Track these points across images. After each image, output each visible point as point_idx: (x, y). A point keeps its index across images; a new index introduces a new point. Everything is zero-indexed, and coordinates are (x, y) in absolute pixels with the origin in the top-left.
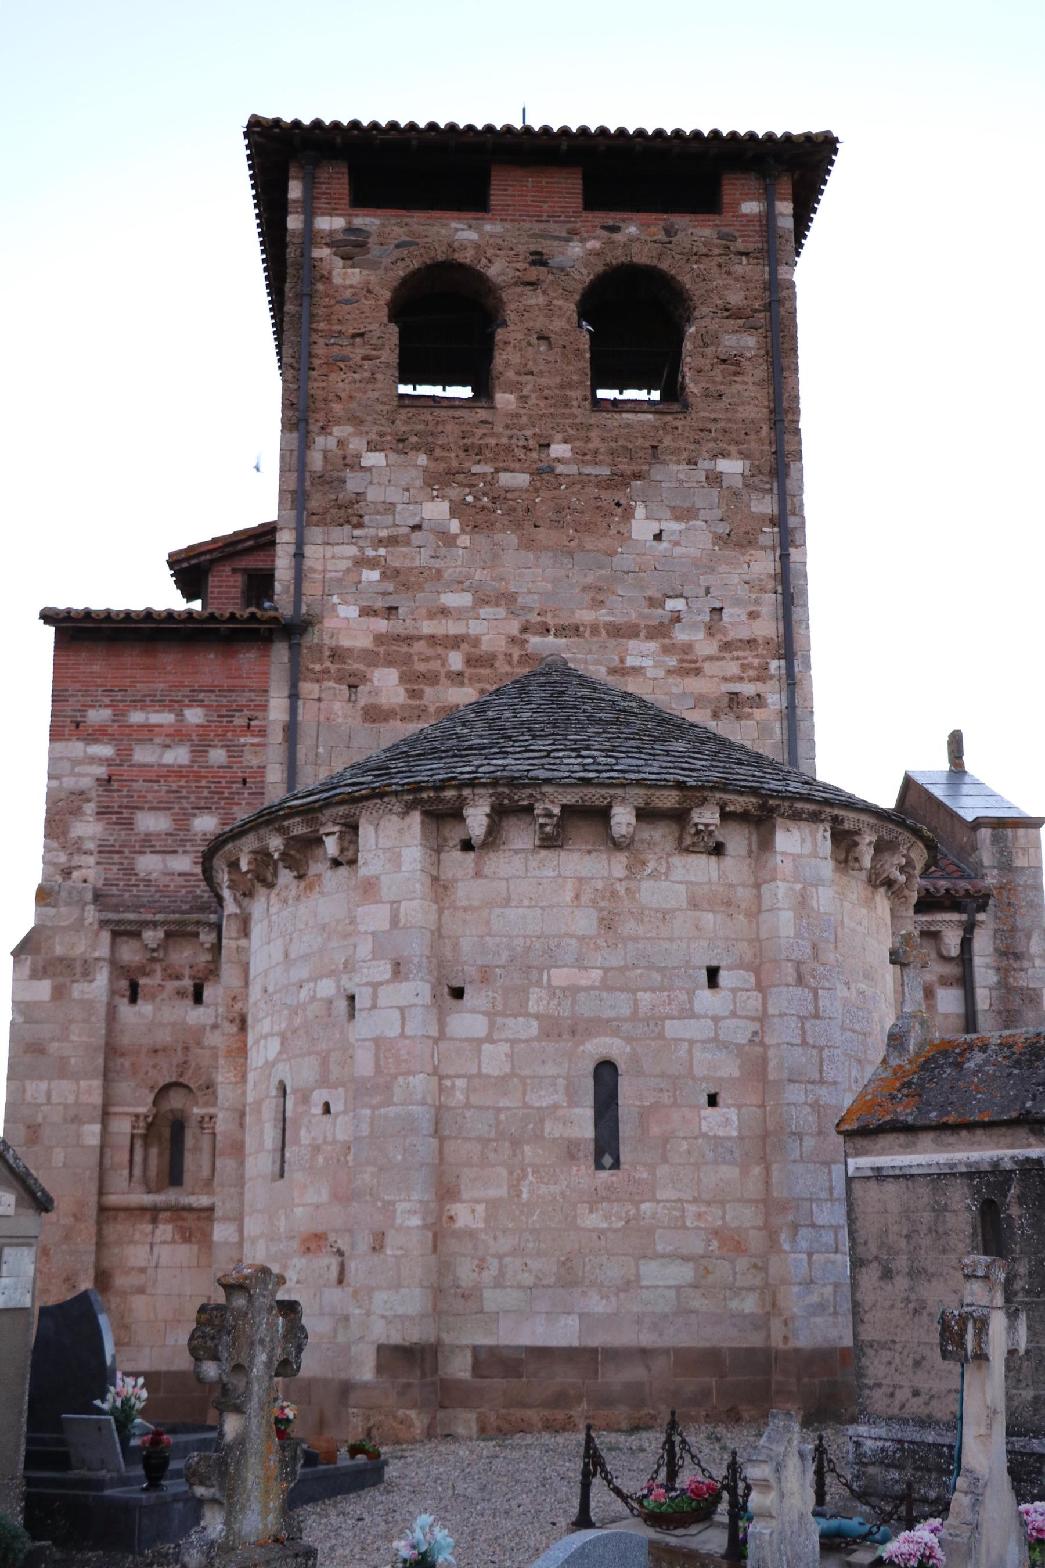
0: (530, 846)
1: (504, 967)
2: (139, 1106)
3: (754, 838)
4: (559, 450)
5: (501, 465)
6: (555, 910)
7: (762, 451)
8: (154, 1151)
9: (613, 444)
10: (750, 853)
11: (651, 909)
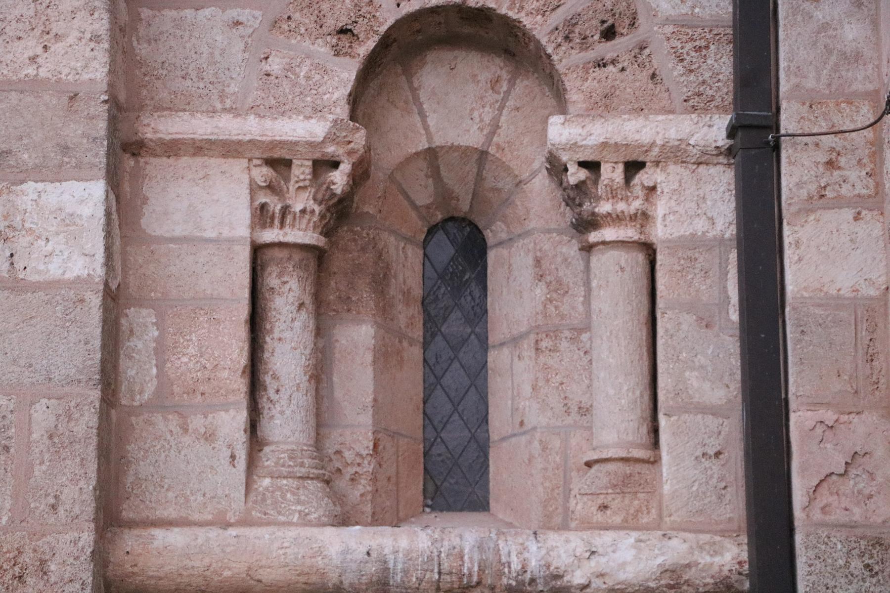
2: (280, 110)
8: (358, 337)
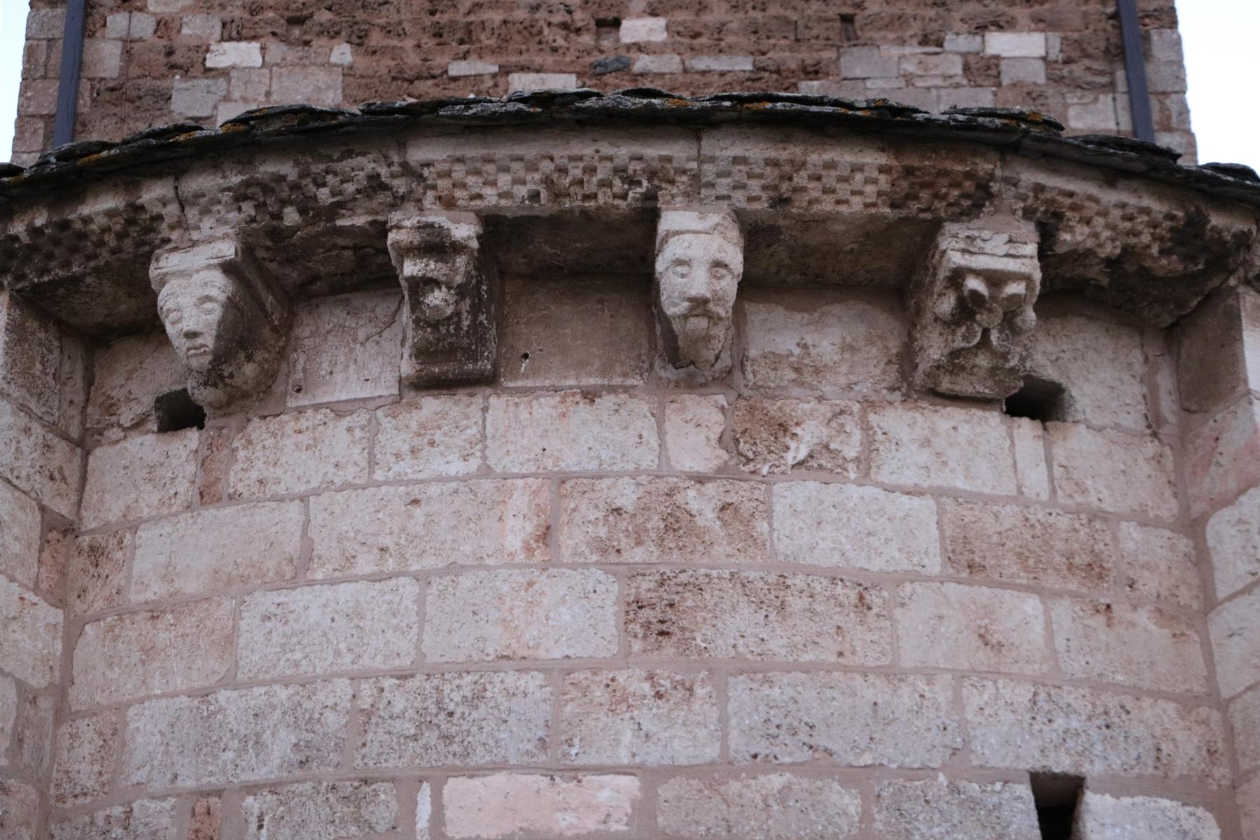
0: (387, 388)
1: (273, 787)
3: (1165, 380)
4: (639, 28)
5: (514, 59)
6: (466, 582)
7: (1085, 15)
9: (757, 15)
10: (1154, 425)
11: (810, 571)
